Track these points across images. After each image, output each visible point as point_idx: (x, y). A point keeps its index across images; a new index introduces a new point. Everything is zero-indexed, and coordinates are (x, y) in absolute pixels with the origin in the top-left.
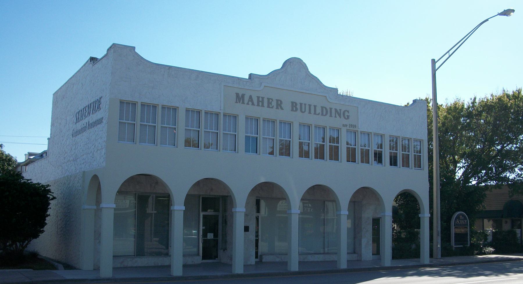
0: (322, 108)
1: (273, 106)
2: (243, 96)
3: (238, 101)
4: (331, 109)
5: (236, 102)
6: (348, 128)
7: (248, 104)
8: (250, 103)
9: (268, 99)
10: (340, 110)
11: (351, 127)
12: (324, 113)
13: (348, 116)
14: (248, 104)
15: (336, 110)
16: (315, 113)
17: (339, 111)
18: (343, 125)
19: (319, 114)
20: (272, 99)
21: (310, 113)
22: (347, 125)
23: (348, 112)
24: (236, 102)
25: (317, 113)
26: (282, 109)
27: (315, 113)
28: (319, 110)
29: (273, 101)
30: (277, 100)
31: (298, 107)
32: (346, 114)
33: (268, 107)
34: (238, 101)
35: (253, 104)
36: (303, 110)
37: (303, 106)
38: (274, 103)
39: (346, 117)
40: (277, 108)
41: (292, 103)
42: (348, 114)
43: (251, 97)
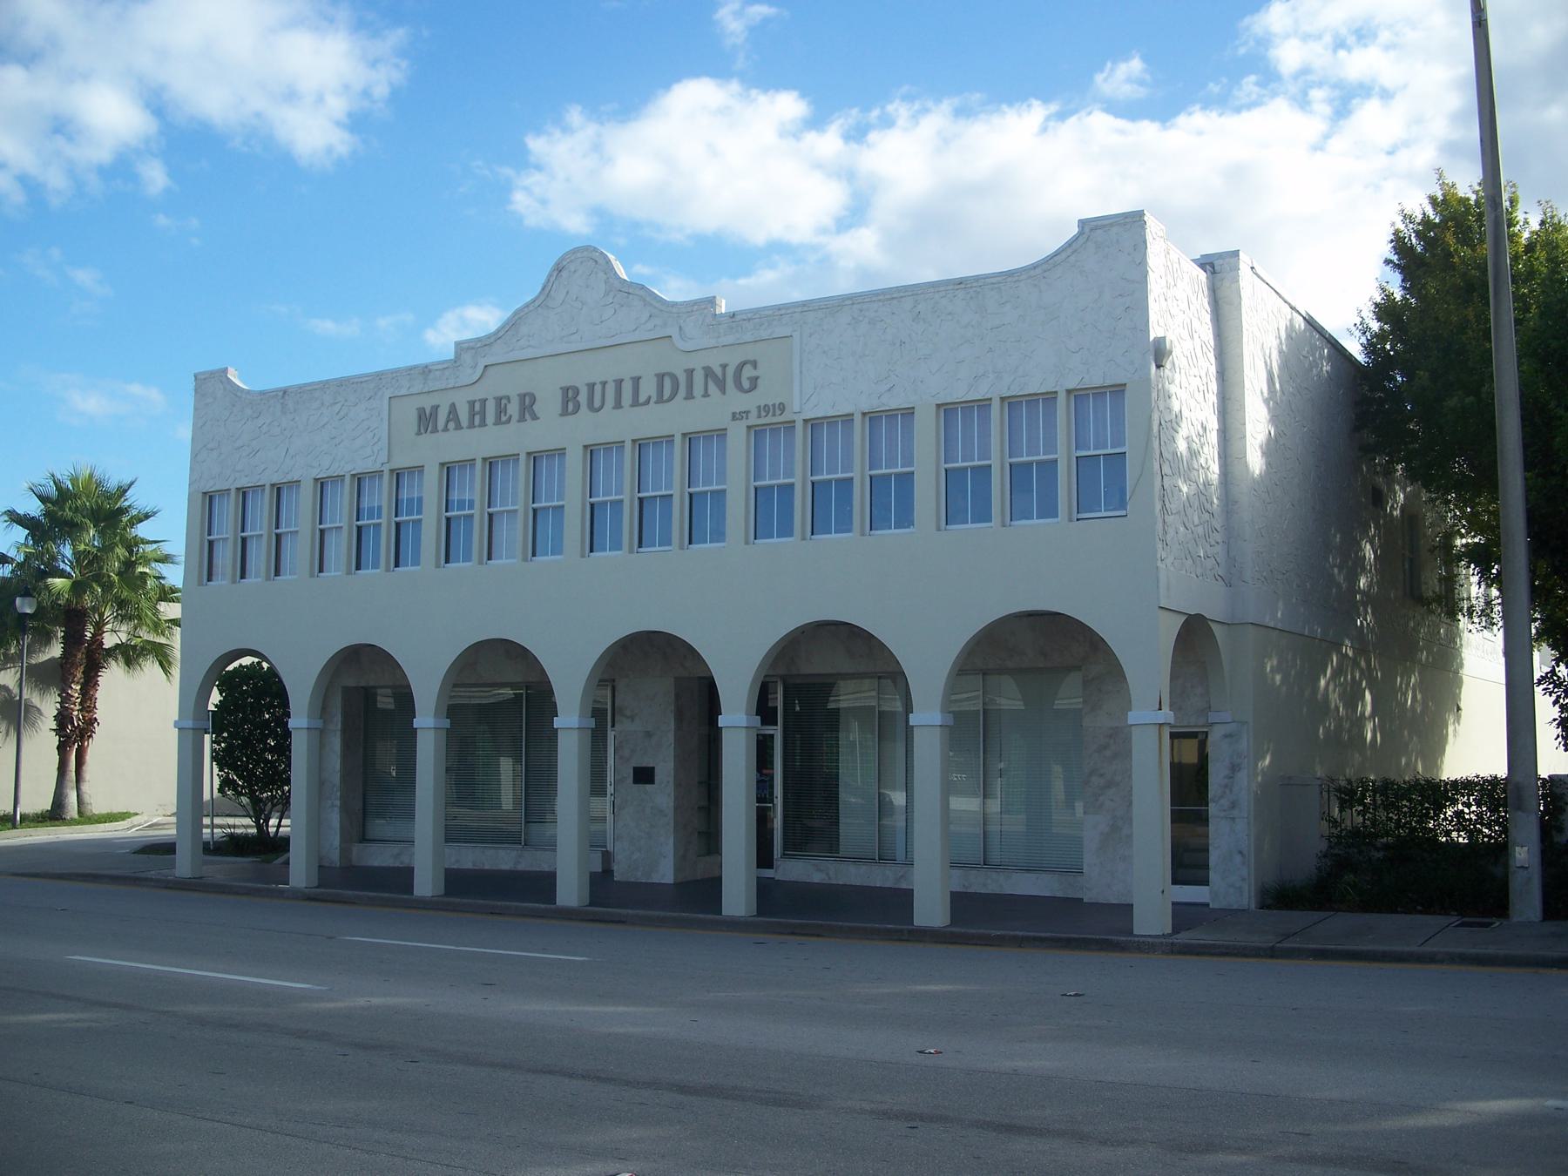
0: (661, 377)
1: (511, 416)
2: (436, 408)
3: (422, 431)
4: (690, 373)
5: (419, 433)
6: (753, 420)
7: (446, 429)
8: (451, 425)
9: (499, 400)
10: (724, 367)
11: (763, 414)
12: (667, 393)
13: (754, 381)
14: (446, 429)
15: (708, 372)
16: (636, 403)
17: (718, 371)
18: (734, 417)
19: (647, 402)
20: (508, 399)
21: (618, 405)
22: (747, 412)
23: (755, 364)
24: (419, 433)
25: (642, 399)
26: (535, 417)
27: (636, 403)
28: (648, 389)
29: (509, 402)
30: (522, 397)
31: (583, 398)
32: (748, 372)
33: (498, 422)
34: (422, 431)
35: (459, 427)
36: (597, 404)
37: (598, 388)
38: (513, 409)
39: (746, 384)
40: (522, 419)
41: (565, 390)
42: (753, 373)
43: (453, 408)
